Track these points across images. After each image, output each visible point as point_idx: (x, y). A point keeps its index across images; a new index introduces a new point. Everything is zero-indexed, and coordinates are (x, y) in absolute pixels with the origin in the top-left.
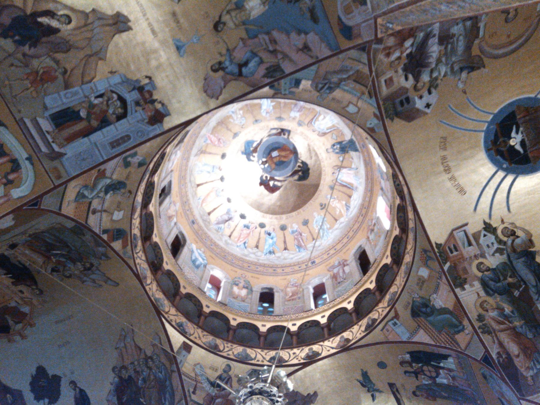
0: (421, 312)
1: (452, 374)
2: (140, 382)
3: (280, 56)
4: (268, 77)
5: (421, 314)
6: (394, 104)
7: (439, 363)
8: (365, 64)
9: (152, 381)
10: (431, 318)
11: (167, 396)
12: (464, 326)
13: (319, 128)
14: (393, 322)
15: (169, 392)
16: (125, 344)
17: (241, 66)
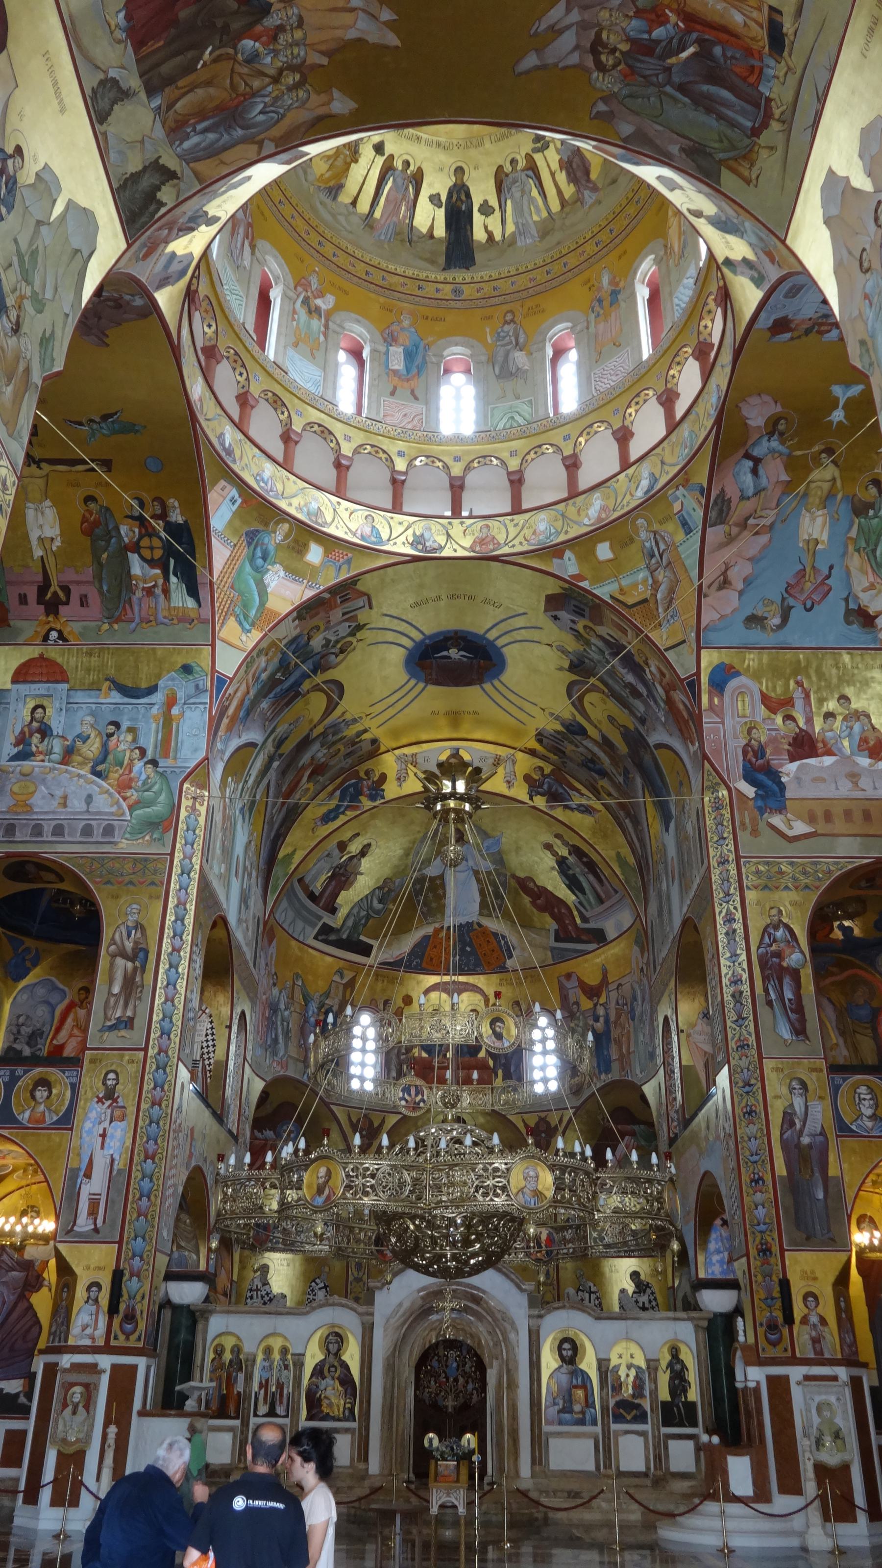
0: (255, 548)
1: (158, 591)
2: (251, 43)
3: (735, 530)
4: (718, 496)
5: (252, 547)
6: (586, 604)
7: (175, 574)
8: (666, 650)
9: (246, 84)
10: (248, 568)
11: (211, 136)
12: (249, 631)
13: (515, 182)
14: (237, 496)
15: (218, 140)
16: (353, 10)
17: (757, 461)
